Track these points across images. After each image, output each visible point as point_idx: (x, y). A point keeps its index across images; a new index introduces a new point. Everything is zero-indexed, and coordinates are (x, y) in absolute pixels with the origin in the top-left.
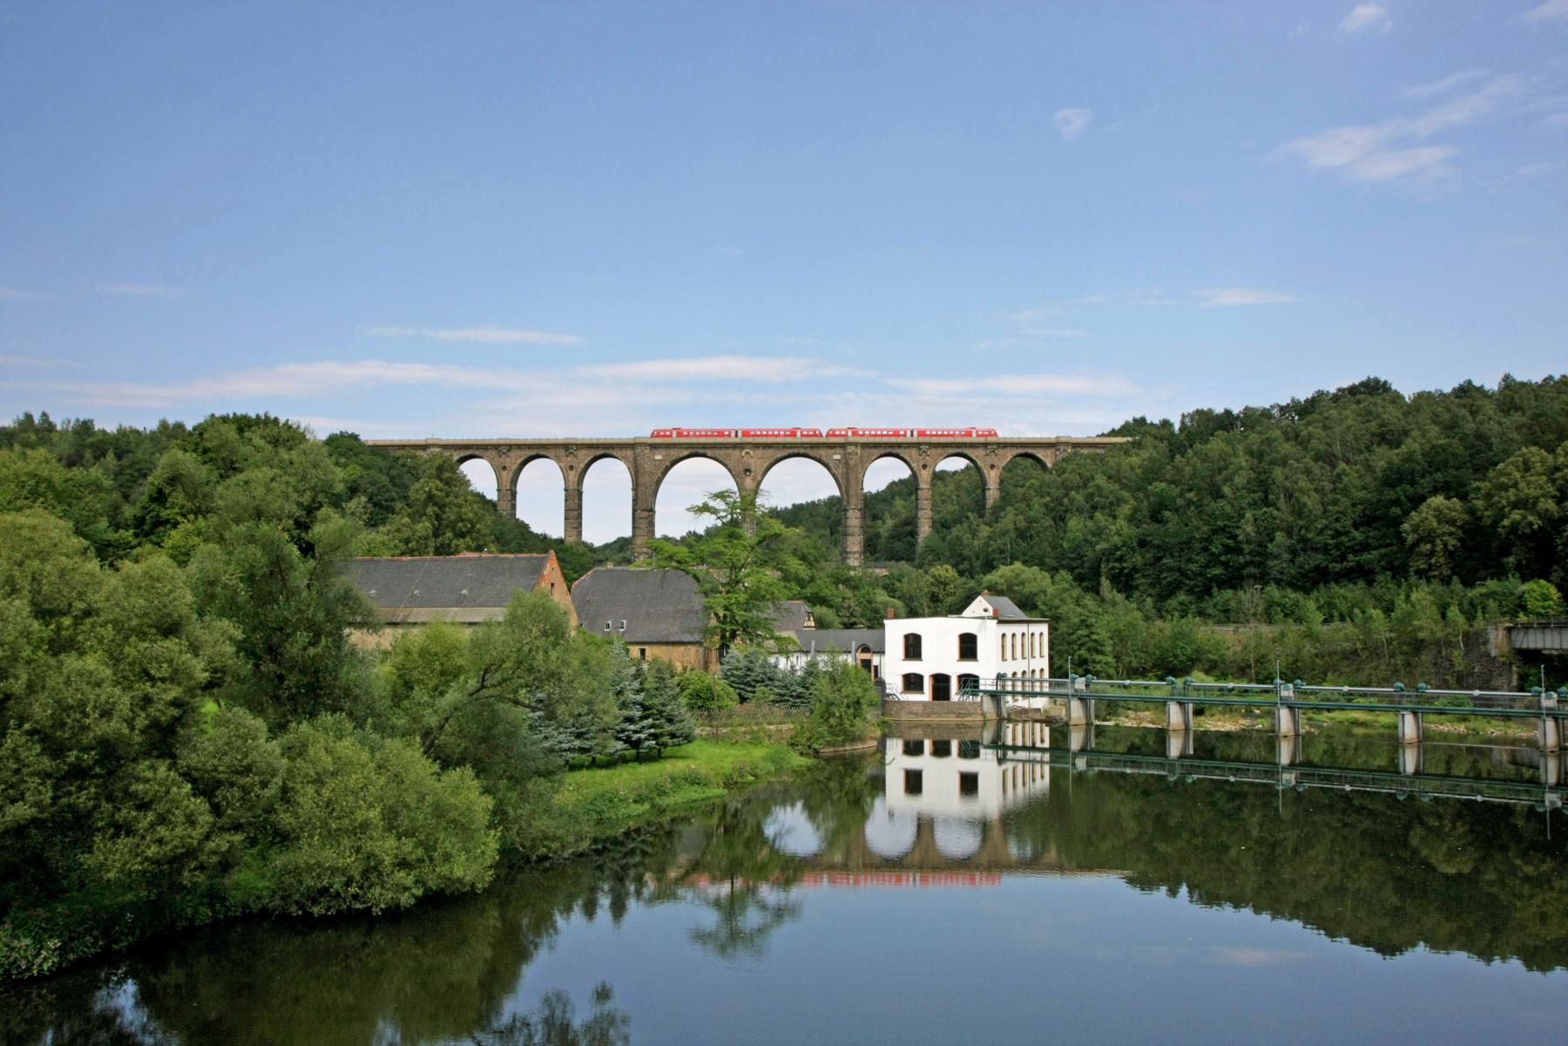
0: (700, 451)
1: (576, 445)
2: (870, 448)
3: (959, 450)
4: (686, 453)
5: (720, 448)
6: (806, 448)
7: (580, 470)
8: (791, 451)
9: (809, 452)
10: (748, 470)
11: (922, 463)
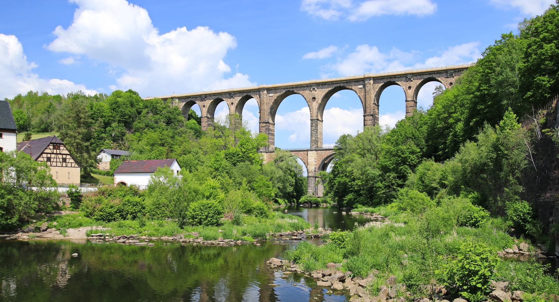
0: (291, 90)
1: (234, 92)
2: (378, 79)
3: (431, 76)
4: (284, 91)
5: (301, 87)
6: (344, 83)
7: (236, 104)
8: (336, 85)
9: (345, 85)
10: (314, 98)
11: (408, 85)
